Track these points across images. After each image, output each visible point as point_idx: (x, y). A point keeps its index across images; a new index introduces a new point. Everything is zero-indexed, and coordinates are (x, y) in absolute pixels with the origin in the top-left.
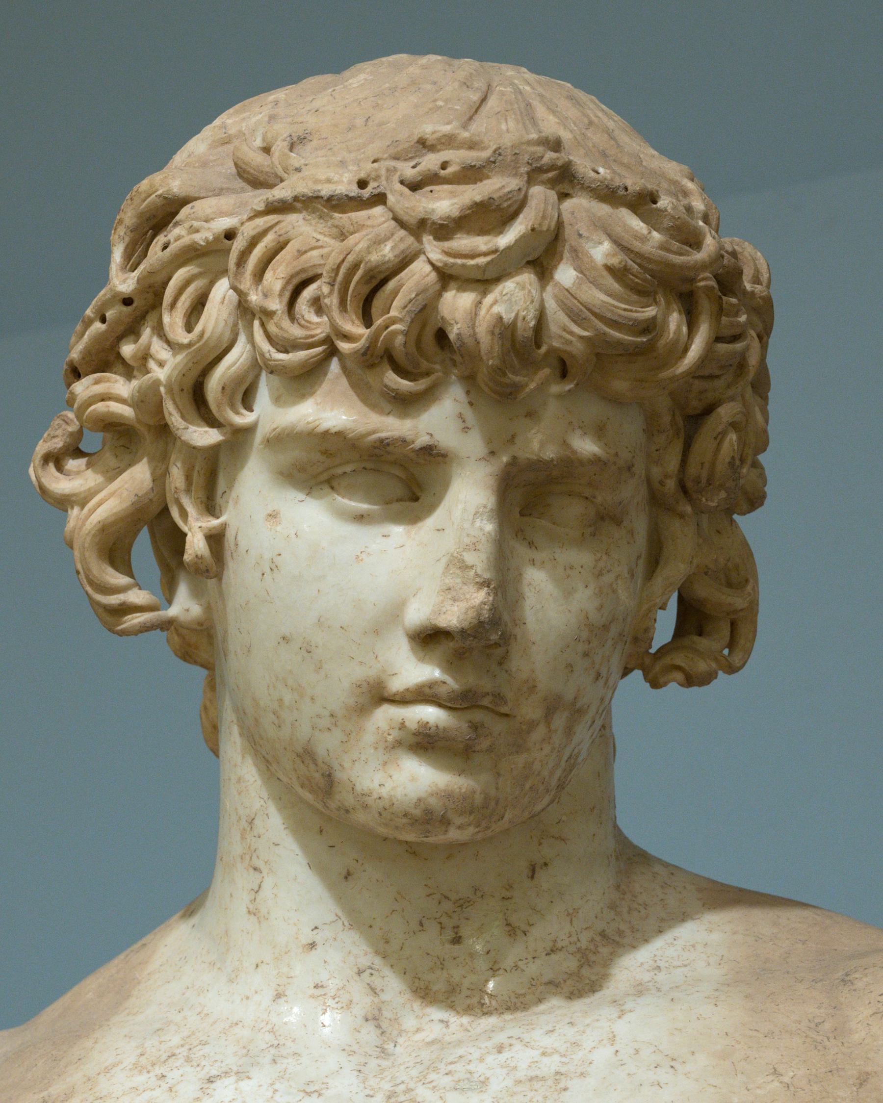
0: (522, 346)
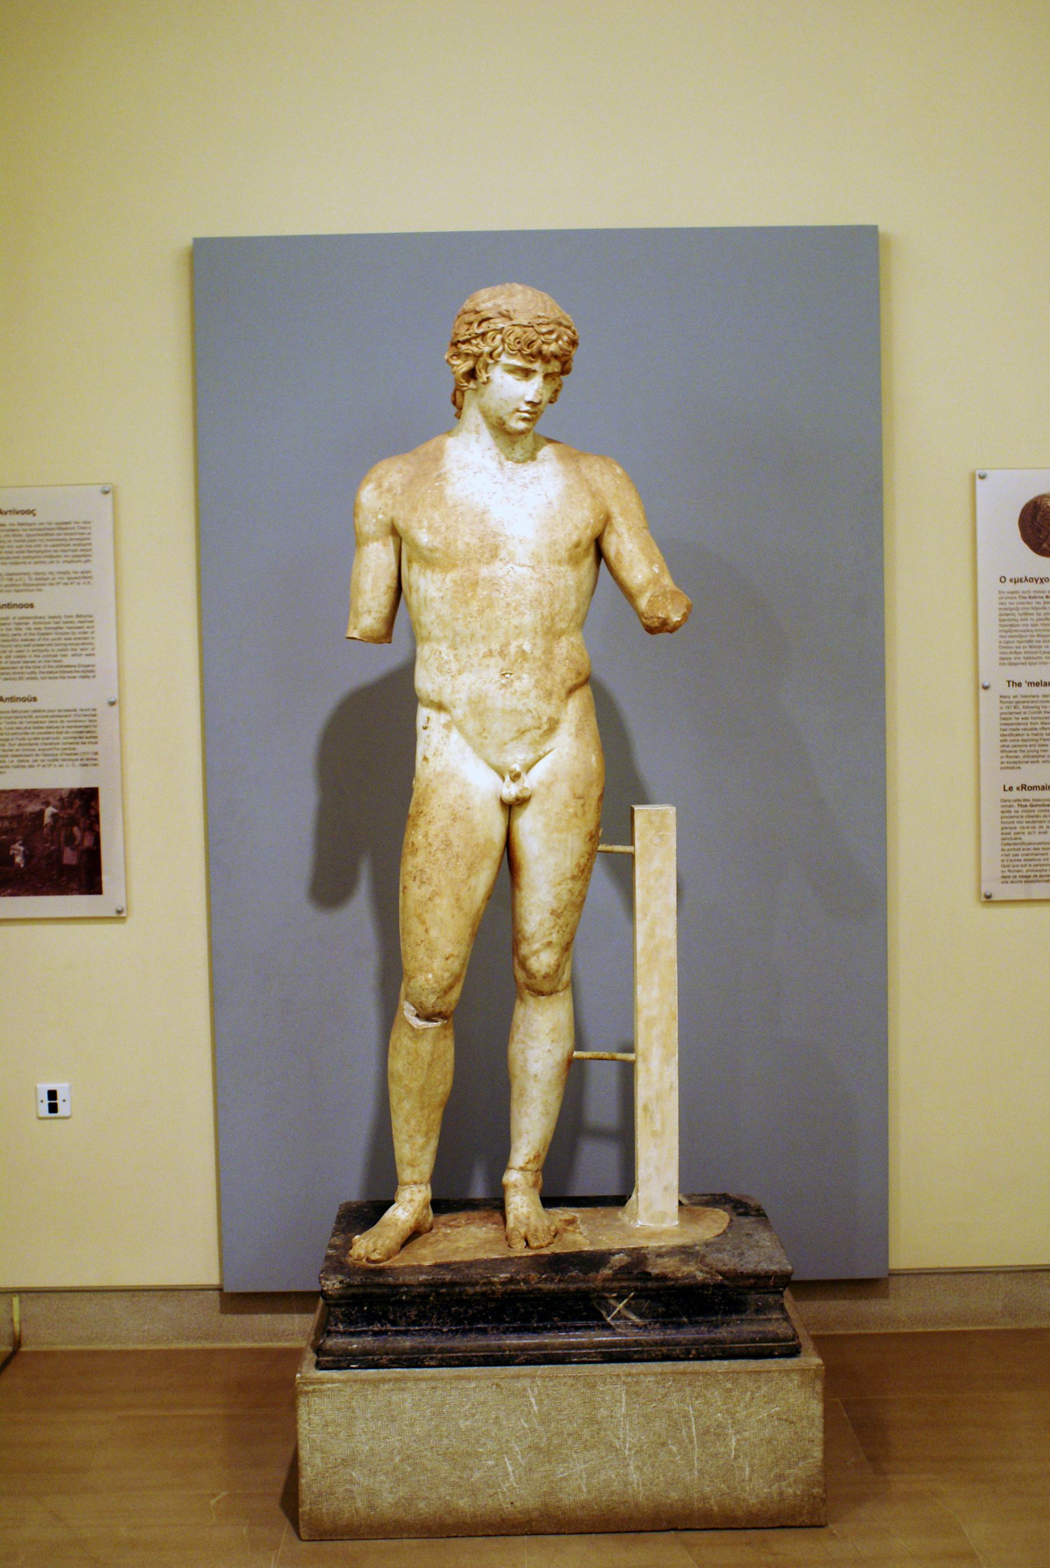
0: (555, 356)
